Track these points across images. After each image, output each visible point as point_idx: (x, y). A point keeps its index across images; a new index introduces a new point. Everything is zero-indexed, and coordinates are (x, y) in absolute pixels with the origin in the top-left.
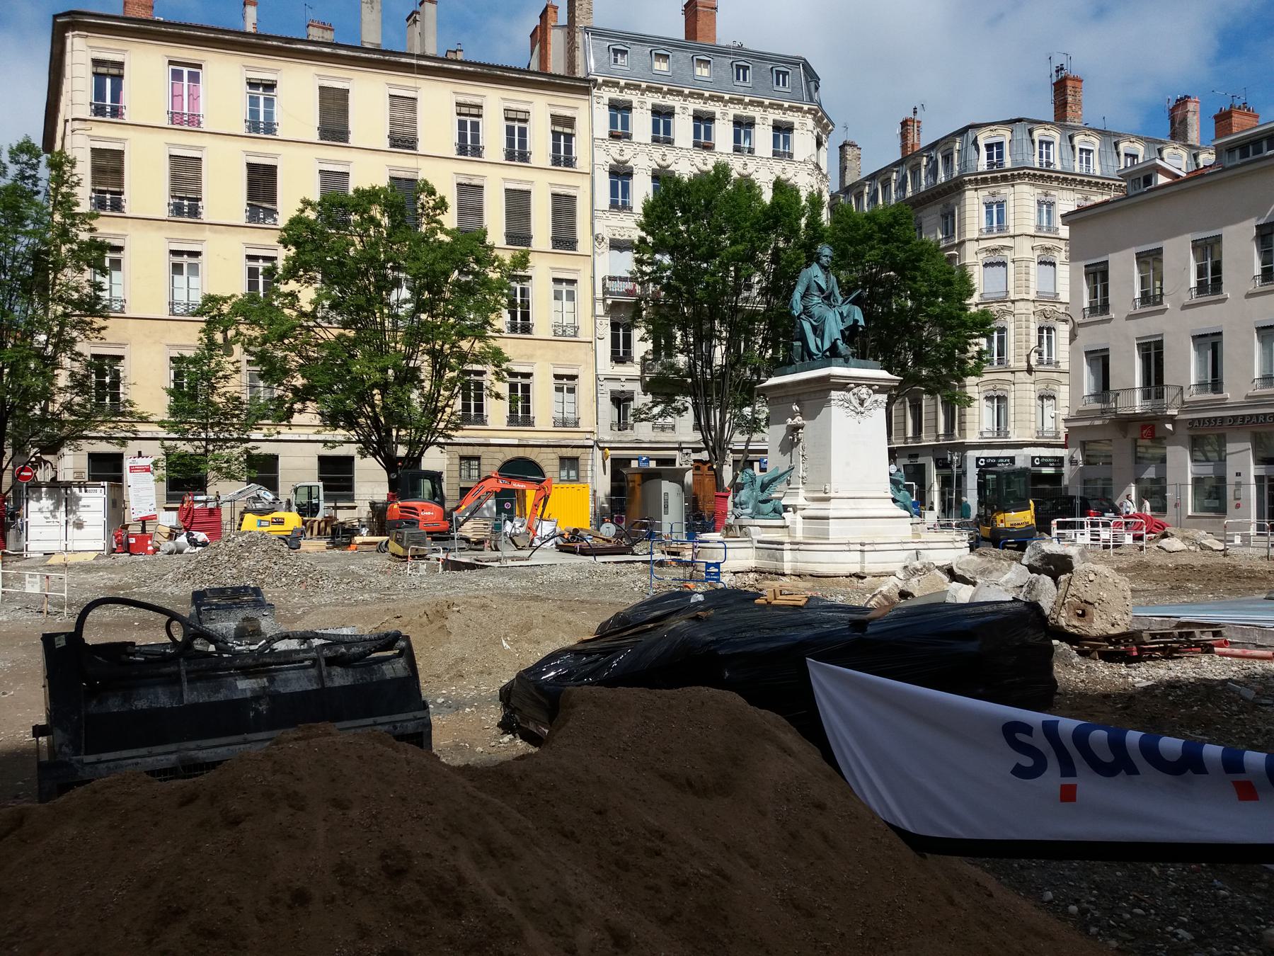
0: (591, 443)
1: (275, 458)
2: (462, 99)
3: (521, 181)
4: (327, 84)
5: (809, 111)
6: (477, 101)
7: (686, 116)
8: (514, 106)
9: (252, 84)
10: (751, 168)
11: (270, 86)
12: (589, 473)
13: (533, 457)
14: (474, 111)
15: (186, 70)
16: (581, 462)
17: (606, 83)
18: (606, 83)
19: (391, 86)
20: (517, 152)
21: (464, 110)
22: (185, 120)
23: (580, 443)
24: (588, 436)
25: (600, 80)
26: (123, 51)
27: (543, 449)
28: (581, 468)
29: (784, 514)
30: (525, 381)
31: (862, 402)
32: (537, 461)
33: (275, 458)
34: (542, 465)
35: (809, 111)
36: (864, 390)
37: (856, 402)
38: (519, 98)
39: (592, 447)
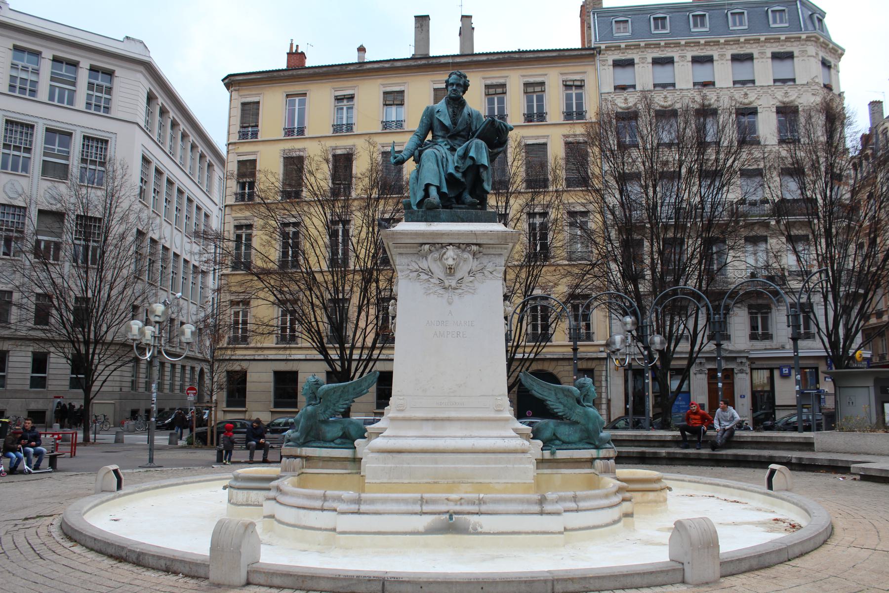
0: (604, 355)
1: (295, 373)
2: (489, 82)
3: (538, 137)
4: (389, 89)
5: (808, 39)
6: (502, 81)
7: (685, 63)
8: (531, 80)
9: (338, 99)
10: (752, 96)
11: (351, 98)
12: (604, 384)
13: (550, 370)
14: (499, 90)
15: (297, 99)
16: (596, 373)
17: (608, 48)
18: (608, 48)
19: (435, 82)
20: (535, 116)
21: (492, 91)
22: (295, 131)
23: (594, 355)
24: (602, 349)
25: (603, 47)
26: (258, 95)
27: (560, 363)
28: (596, 378)
29: (358, 442)
30: (544, 303)
31: (451, 271)
32: (555, 372)
33: (295, 373)
34: (559, 376)
35: (808, 39)
36: (451, 253)
37: (438, 271)
38: (534, 74)
39: (606, 359)
